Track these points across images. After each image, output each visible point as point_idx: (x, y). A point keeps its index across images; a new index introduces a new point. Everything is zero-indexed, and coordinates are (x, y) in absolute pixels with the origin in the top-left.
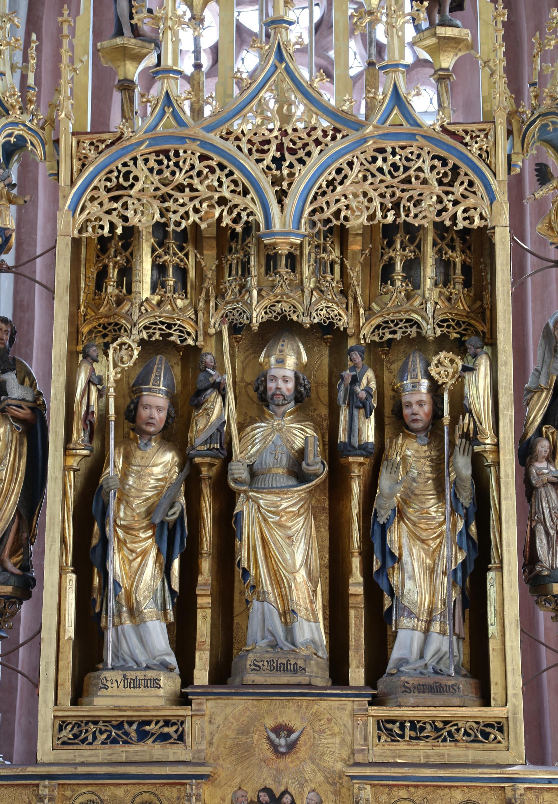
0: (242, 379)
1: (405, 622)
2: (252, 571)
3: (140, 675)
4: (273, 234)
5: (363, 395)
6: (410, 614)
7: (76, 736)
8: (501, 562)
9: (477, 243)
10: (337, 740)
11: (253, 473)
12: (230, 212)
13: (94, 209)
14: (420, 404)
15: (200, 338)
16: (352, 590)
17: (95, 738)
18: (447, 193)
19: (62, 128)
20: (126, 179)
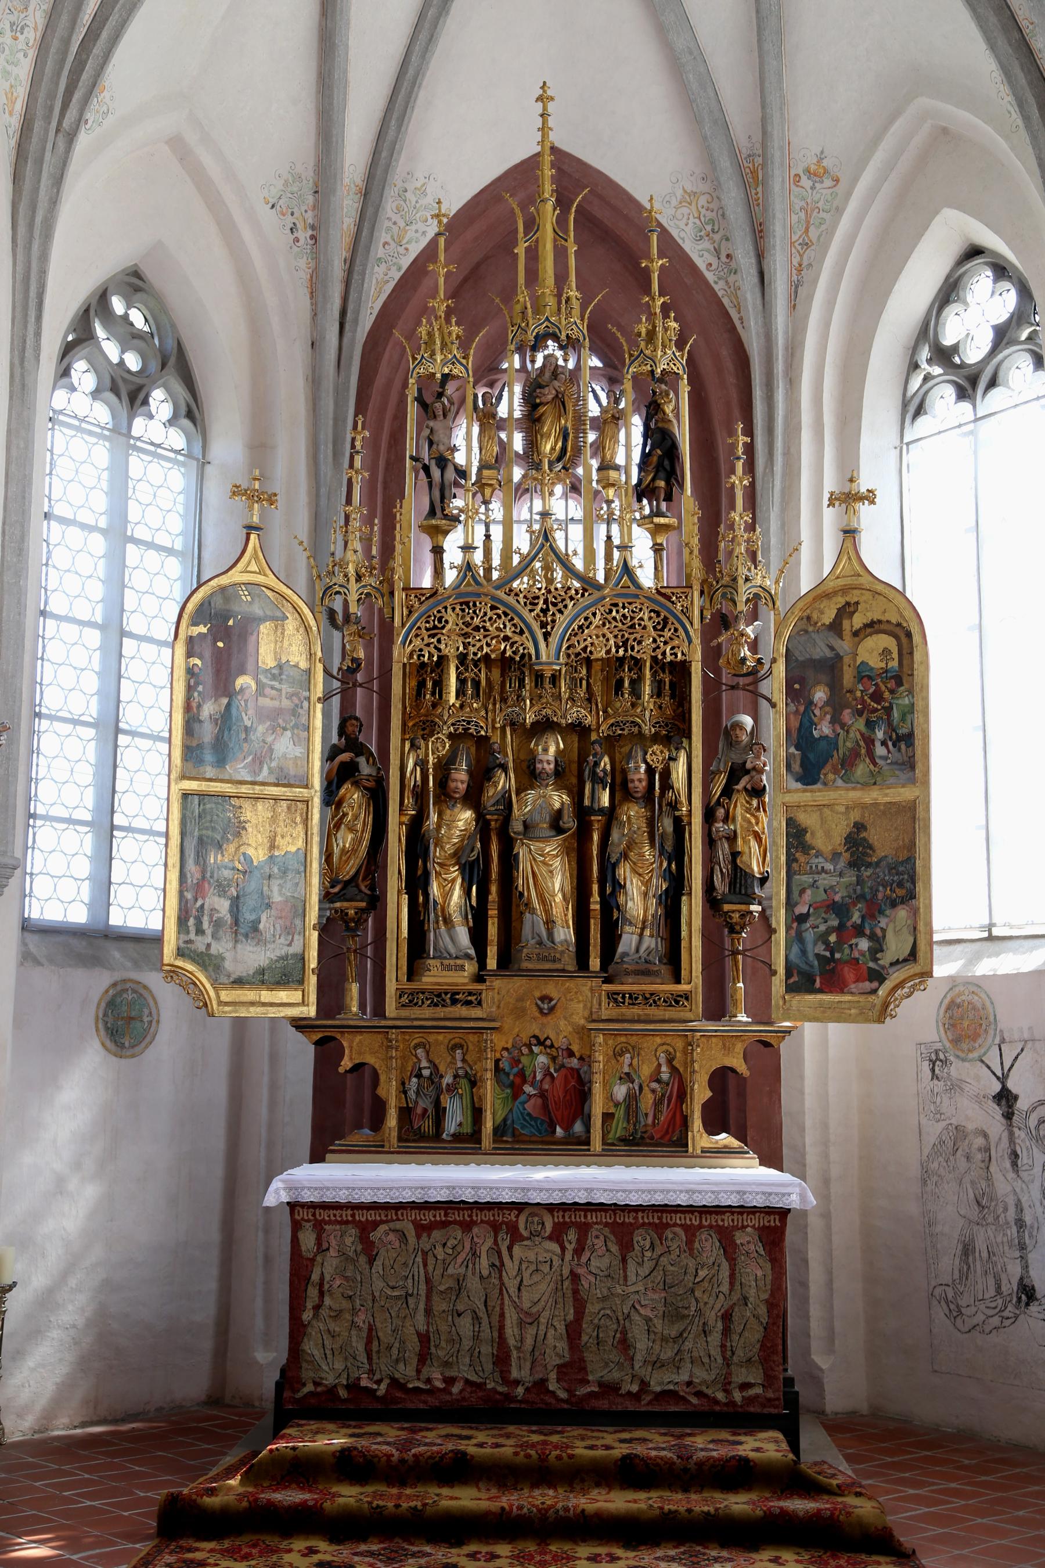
0: (518, 758)
1: (627, 928)
2: (526, 894)
4: (541, 664)
5: (601, 774)
6: (631, 924)
7: (410, 1001)
8: (691, 889)
9: (681, 670)
10: (581, 1005)
11: (526, 826)
12: (512, 646)
13: (418, 642)
14: (640, 780)
15: (490, 731)
16: (592, 907)
17: (423, 1003)
18: (660, 636)
19: (396, 587)
20: (440, 621)
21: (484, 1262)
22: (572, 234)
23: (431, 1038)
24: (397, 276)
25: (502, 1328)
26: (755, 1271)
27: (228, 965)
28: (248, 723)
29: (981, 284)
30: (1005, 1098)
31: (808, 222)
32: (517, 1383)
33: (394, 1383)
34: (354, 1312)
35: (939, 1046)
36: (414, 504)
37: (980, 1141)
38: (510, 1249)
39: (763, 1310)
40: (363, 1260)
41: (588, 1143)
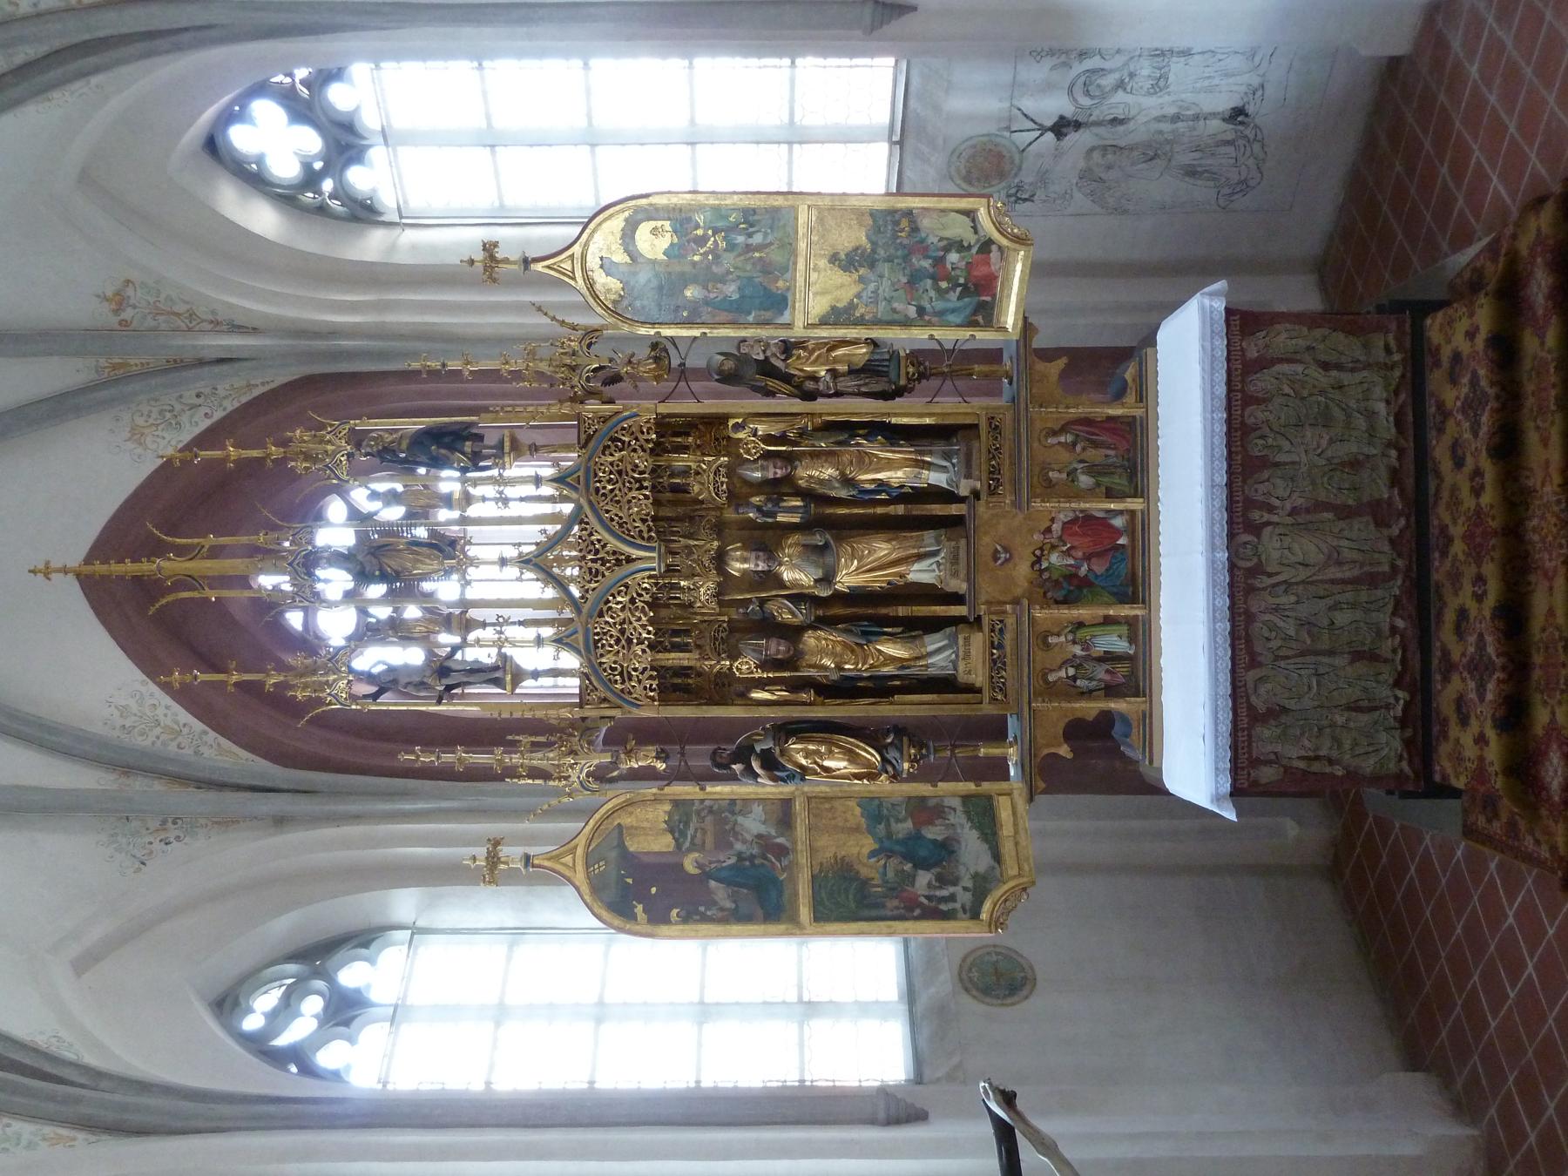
3: (961, 650)
9: (664, 425)
21: (1283, 600)
22: (196, 541)
23: (1039, 667)
24: (212, 734)
25: (1343, 582)
26: (1282, 339)
27: (982, 869)
28: (733, 860)
30: (1061, 127)
31: (169, 313)
32: (1394, 567)
33: (1398, 684)
34: (1333, 725)
35: (1003, 193)
36: (475, 703)
37: (1096, 155)
38: (1270, 575)
39: (1318, 333)
40: (1284, 719)
41: (1132, 513)
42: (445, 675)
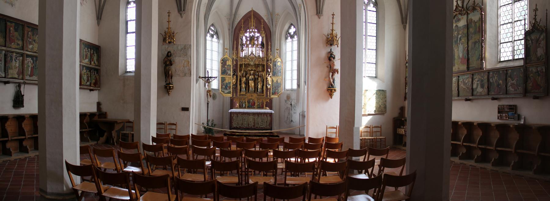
26: (269, 118)
29: (293, 27)
42: (242, 45)
